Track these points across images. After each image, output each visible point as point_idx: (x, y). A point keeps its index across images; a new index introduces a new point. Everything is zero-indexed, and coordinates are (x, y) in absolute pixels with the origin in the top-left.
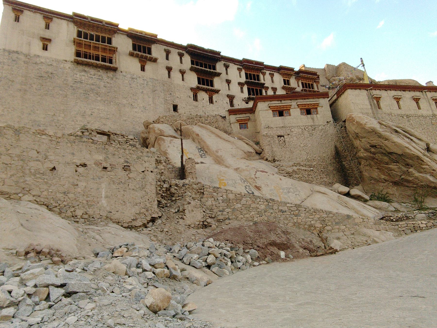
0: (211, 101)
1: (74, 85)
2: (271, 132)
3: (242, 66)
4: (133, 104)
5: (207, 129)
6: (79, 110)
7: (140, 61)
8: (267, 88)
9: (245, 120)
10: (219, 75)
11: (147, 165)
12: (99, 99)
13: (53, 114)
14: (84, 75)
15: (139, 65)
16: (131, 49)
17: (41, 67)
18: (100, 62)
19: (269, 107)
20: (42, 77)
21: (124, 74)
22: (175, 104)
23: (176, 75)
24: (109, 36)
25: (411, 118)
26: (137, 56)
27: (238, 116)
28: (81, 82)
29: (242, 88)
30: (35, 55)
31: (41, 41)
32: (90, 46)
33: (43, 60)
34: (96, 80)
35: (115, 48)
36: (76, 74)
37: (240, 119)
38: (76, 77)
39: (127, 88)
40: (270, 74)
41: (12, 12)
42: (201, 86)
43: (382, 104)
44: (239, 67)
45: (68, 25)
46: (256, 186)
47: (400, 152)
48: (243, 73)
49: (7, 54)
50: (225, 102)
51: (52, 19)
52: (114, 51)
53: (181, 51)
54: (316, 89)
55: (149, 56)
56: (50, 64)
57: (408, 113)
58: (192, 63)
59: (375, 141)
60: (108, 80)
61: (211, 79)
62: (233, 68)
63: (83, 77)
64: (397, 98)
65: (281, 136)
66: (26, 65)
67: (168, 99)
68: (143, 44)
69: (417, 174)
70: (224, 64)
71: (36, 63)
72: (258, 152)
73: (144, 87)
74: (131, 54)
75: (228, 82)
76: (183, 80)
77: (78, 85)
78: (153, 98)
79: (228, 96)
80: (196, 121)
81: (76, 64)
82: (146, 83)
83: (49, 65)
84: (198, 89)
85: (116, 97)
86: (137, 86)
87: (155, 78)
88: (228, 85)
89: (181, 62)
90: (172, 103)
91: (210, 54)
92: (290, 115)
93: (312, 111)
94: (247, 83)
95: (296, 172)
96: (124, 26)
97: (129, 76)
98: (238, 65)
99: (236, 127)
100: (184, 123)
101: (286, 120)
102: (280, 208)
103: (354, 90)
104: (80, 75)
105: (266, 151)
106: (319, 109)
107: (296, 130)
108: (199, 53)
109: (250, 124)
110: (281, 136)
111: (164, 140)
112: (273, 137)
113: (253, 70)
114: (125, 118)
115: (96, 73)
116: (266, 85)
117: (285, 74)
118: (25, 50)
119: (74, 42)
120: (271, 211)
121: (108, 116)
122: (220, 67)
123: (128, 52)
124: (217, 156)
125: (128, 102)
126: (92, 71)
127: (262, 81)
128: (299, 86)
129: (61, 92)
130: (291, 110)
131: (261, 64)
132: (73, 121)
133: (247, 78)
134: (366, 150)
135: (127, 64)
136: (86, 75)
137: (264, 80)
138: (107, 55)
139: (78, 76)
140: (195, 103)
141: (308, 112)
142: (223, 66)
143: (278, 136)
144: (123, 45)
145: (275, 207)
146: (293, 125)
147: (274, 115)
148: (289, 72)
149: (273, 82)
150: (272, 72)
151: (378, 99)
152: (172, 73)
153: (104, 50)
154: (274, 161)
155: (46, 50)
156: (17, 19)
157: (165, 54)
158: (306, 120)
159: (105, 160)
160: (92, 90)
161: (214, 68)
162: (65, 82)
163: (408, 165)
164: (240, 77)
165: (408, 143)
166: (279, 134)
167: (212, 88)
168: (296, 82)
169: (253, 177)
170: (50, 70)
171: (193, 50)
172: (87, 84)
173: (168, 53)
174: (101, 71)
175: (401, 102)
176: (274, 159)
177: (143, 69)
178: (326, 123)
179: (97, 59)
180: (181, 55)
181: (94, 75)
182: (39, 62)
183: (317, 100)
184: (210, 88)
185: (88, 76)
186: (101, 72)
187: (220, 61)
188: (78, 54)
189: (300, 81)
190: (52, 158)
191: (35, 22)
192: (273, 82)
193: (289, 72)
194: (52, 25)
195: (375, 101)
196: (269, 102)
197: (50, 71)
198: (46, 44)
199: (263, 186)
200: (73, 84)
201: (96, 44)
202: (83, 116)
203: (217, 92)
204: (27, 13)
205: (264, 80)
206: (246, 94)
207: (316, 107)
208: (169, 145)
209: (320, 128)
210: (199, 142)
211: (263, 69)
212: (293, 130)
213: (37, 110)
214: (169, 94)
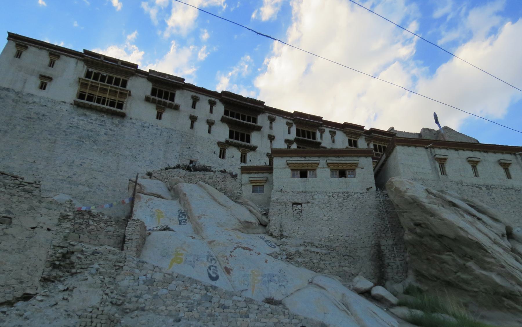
1: (68, 130)
3: (293, 120)
4: (137, 157)
9: (261, 181)
10: (259, 129)
11: (41, 219)
12: (95, 147)
13: (33, 161)
14: (83, 120)
15: (155, 112)
16: (149, 93)
17: (33, 108)
18: (95, 104)
19: (288, 164)
20: (30, 118)
21: (134, 121)
23: (201, 127)
24: (125, 78)
25: (494, 190)
26: (153, 102)
27: (253, 175)
28: (77, 128)
30: (28, 94)
32: (97, 87)
34: (96, 125)
36: (74, 118)
37: (255, 179)
38: (72, 121)
39: (133, 137)
40: (330, 132)
41: (48, 57)
43: (448, 168)
44: (289, 121)
45: (77, 63)
46: (226, 268)
47: (452, 235)
48: (294, 129)
53: (213, 99)
57: (490, 182)
58: (226, 113)
59: (419, 217)
60: (112, 127)
61: (248, 134)
62: (280, 124)
63: (81, 123)
64: (473, 161)
65: (297, 204)
66: (14, 104)
67: (184, 153)
69: (478, 271)
70: (269, 117)
71: (27, 103)
72: (263, 223)
73: (156, 137)
74: (147, 99)
75: (271, 138)
76: (209, 132)
77: (73, 130)
80: (196, 180)
82: (159, 133)
83: (43, 106)
84: (228, 144)
85: (118, 147)
86: (148, 135)
88: (271, 142)
89: (211, 111)
91: (249, 104)
92: (316, 177)
93: (347, 172)
94: (296, 140)
95: (300, 253)
97: (140, 124)
98: (288, 119)
99: (247, 191)
102: (222, 301)
103: (406, 147)
104: (78, 120)
105: (272, 222)
106: (358, 171)
108: (236, 102)
109: (266, 187)
111: (140, 198)
112: (285, 204)
114: (123, 173)
115: (99, 118)
117: (352, 133)
118: (18, 87)
120: (208, 304)
121: (102, 168)
122: (262, 120)
123: (144, 98)
124: (197, 223)
125: (131, 154)
126: (94, 116)
127: (318, 140)
129: (49, 137)
130: (318, 171)
131: (320, 119)
132: (56, 171)
133: (298, 134)
134: (411, 231)
136: (85, 120)
137: (321, 138)
138: (117, 99)
141: (342, 174)
143: (293, 204)
144: (139, 88)
145: (215, 300)
147: (293, 176)
148: (357, 131)
149: (333, 141)
150: (333, 130)
151: (442, 161)
152: (196, 124)
154: (282, 236)
157: (191, 102)
160: (89, 137)
161: (255, 121)
162: (57, 126)
163: (465, 256)
164: (289, 133)
165: (471, 223)
166: (296, 201)
167: (247, 144)
171: (227, 98)
172: (84, 130)
173: (195, 100)
174: (105, 116)
175: (479, 167)
176: (282, 235)
178: (365, 190)
180: (212, 104)
181: (96, 120)
182: (31, 102)
184: (244, 143)
185: (87, 121)
186: (105, 118)
187: (263, 113)
188: (81, 96)
189: (372, 143)
192: (333, 141)
193: (357, 131)
195: (437, 165)
196: (288, 158)
197: (43, 112)
200: (68, 129)
202: (70, 166)
203: (254, 149)
205: (321, 138)
207: (352, 168)
209: (356, 196)
210: (184, 205)
211: (321, 125)
212: (315, 197)
213: (15, 155)
214: (187, 148)
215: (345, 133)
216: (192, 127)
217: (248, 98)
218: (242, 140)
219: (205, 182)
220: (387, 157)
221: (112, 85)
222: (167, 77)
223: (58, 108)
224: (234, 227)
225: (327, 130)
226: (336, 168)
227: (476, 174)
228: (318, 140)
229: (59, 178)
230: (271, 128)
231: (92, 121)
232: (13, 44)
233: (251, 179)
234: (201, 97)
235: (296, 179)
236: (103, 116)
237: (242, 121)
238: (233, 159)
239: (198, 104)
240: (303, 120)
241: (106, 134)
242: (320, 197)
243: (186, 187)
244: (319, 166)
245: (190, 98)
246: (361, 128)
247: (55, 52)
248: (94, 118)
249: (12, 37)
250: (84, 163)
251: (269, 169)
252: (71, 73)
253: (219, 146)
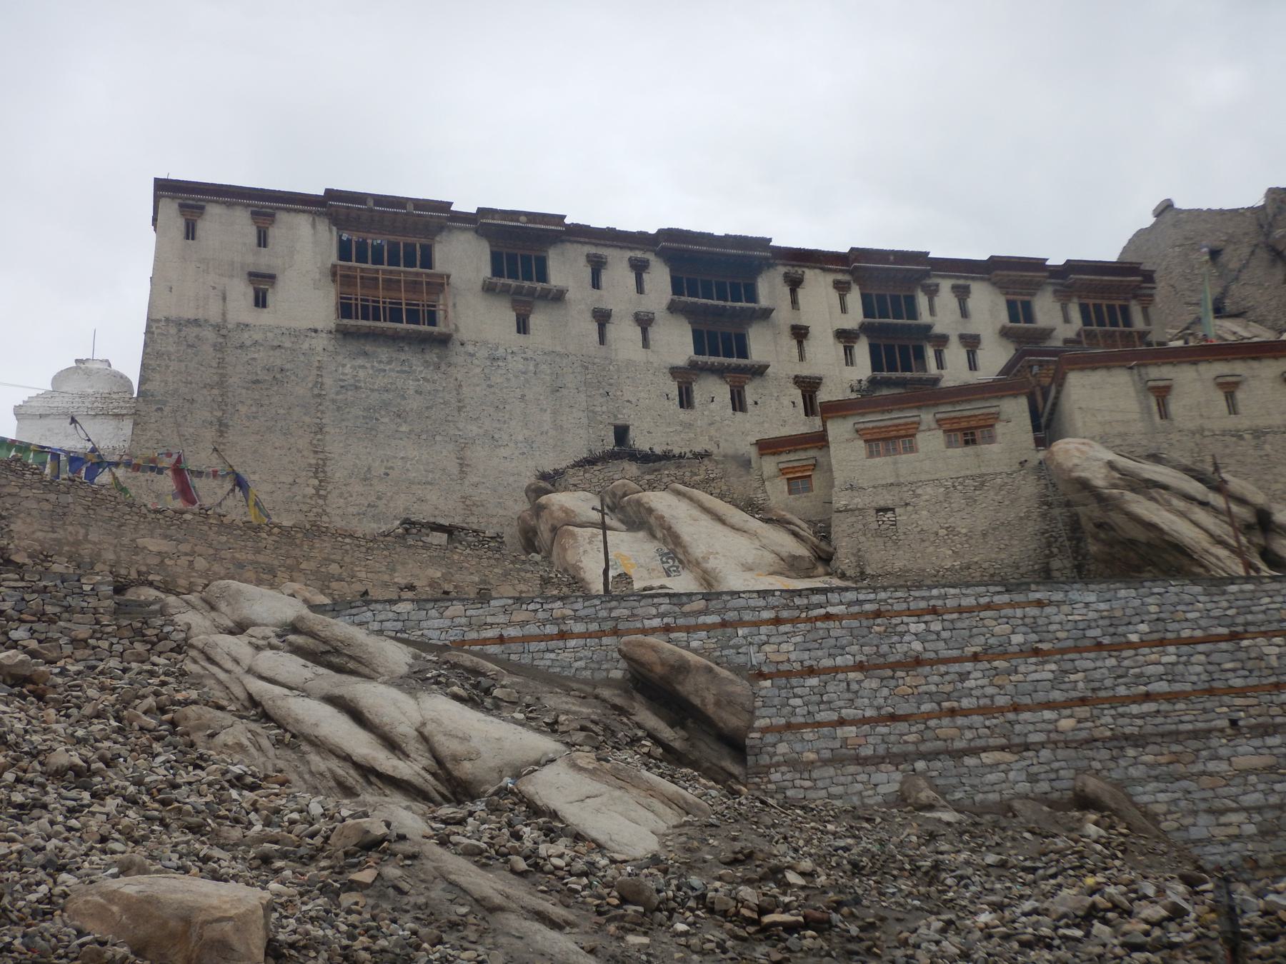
0: (738, 403)
1: (339, 397)
2: (858, 501)
3: (850, 272)
4: (496, 436)
5: (691, 499)
6: (355, 465)
7: (515, 305)
8: (942, 341)
9: (804, 468)
10: (766, 314)
12: (404, 428)
13: (291, 480)
14: (363, 367)
15: (511, 317)
16: (486, 271)
17: (256, 356)
19: (857, 431)
20: (257, 382)
21: (470, 348)
22: (619, 422)
23: (624, 334)
24: (424, 241)
25: (1269, 437)
26: (505, 291)
27: (784, 458)
28: (356, 388)
29: (848, 351)
30: (238, 325)
31: (251, 282)
32: (377, 279)
33: (258, 336)
35: (441, 276)
36: (344, 366)
37: (790, 465)
38: (343, 374)
39: (478, 389)
40: (955, 288)
42: (701, 359)
43: (1174, 406)
44: (840, 277)
45: (314, 226)
48: (854, 298)
49: (173, 331)
50: (786, 402)
51: (273, 215)
52: (439, 284)
53: (639, 254)
54: (1139, 323)
55: (539, 286)
56: (276, 343)
57: (1261, 423)
58: (677, 288)
60: (427, 373)
62: (818, 287)
63: (361, 374)
64: (1228, 383)
65: (885, 510)
67: (598, 409)
68: (524, 248)
70: (786, 276)
71: (242, 346)
73: (527, 381)
74: (489, 289)
75: (800, 333)
76: (646, 343)
78: (554, 413)
79: (799, 381)
80: (665, 480)
81: (339, 336)
82: (532, 368)
85: (450, 418)
86: (508, 380)
87: (558, 349)
88: (800, 343)
89: (640, 289)
90: (612, 420)
93: (978, 433)
94: (865, 329)
96: (465, 204)
97: (483, 353)
98: (835, 271)
99: (777, 494)
100: (633, 485)
101: (903, 465)
103: (1088, 373)
104: (354, 368)
105: (841, 553)
106: (1000, 428)
107: (928, 492)
109: (817, 480)
111: (573, 535)
113: (888, 287)
114: (476, 479)
115: (394, 355)
116: (938, 329)
118: (213, 312)
119: (334, 274)
121: (430, 475)
122: (770, 289)
123: (480, 283)
125: (481, 431)
126: (384, 353)
127: (925, 317)
128: (1067, 320)
129: (307, 419)
130: (919, 436)
131: (921, 257)
132: (341, 495)
133: (867, 312)
134: (1095, 537)
135: (478, 318)
136: (368, 365)
139: (348, 370)
140: (684, 415)
142: (779, 280)
143: (878, 510)
144: (463, 261)
146: (923, 477)
149: (964, 313)
150: (961, 282)
151: (1162, 393)
152: (611, 330)
153: (414, 286)
155: (264, 306)
156: (190, 233)
158: (960, 459)
159: (445, 577)
160: (386, 405)
161: (752, 297)
162: (316, 391)
164: (844, 309)
165: (1182, 514)
166: (882, 504)
167: (742, 362)
168: (1058, 306)
170: (277, 360)
171: (675, 245)
172: (372, 390)
173: (597, 266)
174: (406, 348)
175: (1240, 395)
176: (862, 573)
177: (522, 327)
178: (1018, 466)
179: (395, 316)
180: (639, 268)
181: (389, 362)
182: (248, 343)
183: (995, 403)
185: (373, 367)
188: (345, 309)
189: (1075, 300)
190: (363, 575)
191: (227, 231)
192: (964, 313)
194: (275, 233)
197: (278, 362)
200: (338, 393)
201: (391, 272)
202: (365, 480)
203: (759, 371)
204: (214, 211)
206: (863, 368)
207: (990, 422)
208: (588, 547)
209: (999, 481)
211: (927, 274)
212: (919, 491)
213: (254, 473)
215: (994, 284)
216: (602, 340)
217: (727, 236)
218: (728, 354)
219: (684, 484)
220: (1058, 392)
221: (402, 268)
222: (523, 219)
223: (306, 346)
224: (772, 569)
225: (945, 285)
226: (956, 426)
227: (1233, 409)
228: (925, 317)
229: (351, 510)
230: (794, 303)
231: (382, 366)
232: (170, 208)
233: (782, 466)
234: (609, 253)
235: (877, 460)
237: (721, 303)
238: (712, 406)
239: (605, 277)
240: (877, 269)
241: (418, 392)
242: (929, 490)
243: (661, 502)
244: (922, 428)
245: (582, 261)
246: (1037, 265)
247: (263, 207)
248: (384, 358)
249: (164, 188)
250: (392, 468)
251: (820, 440)
252: (307, 250)
253: (674, 378)
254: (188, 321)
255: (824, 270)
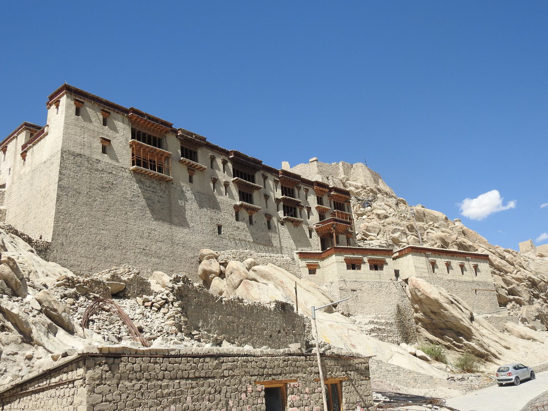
10: (258, 188)
20: (103, 188)
46: (351, 344)
56: (110, 171)
65: (354, 291)
71: (97, 170)
102: (387, 368)
106: (385, 267)
107: (366, 286)
110: (354, 291)
118: (87, 152)
120: (381, 370)
143: (352, 290)
145: (383, 368)
147: (348, 268)
166: (353, 288)
169: (347, 335)
176: (349, 314)
181: (149, 187)
198: (106, 146)
199: (357, 345)
229: (137, 251)
231: (147, 188)
236: (153, 182)
248: (147, 184)
254: (78, 155)
255: (272, 174)
